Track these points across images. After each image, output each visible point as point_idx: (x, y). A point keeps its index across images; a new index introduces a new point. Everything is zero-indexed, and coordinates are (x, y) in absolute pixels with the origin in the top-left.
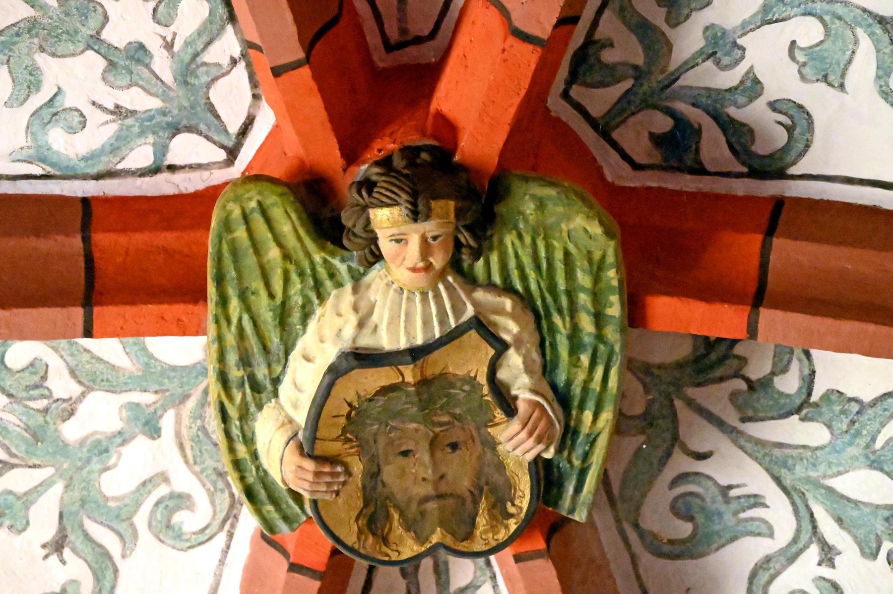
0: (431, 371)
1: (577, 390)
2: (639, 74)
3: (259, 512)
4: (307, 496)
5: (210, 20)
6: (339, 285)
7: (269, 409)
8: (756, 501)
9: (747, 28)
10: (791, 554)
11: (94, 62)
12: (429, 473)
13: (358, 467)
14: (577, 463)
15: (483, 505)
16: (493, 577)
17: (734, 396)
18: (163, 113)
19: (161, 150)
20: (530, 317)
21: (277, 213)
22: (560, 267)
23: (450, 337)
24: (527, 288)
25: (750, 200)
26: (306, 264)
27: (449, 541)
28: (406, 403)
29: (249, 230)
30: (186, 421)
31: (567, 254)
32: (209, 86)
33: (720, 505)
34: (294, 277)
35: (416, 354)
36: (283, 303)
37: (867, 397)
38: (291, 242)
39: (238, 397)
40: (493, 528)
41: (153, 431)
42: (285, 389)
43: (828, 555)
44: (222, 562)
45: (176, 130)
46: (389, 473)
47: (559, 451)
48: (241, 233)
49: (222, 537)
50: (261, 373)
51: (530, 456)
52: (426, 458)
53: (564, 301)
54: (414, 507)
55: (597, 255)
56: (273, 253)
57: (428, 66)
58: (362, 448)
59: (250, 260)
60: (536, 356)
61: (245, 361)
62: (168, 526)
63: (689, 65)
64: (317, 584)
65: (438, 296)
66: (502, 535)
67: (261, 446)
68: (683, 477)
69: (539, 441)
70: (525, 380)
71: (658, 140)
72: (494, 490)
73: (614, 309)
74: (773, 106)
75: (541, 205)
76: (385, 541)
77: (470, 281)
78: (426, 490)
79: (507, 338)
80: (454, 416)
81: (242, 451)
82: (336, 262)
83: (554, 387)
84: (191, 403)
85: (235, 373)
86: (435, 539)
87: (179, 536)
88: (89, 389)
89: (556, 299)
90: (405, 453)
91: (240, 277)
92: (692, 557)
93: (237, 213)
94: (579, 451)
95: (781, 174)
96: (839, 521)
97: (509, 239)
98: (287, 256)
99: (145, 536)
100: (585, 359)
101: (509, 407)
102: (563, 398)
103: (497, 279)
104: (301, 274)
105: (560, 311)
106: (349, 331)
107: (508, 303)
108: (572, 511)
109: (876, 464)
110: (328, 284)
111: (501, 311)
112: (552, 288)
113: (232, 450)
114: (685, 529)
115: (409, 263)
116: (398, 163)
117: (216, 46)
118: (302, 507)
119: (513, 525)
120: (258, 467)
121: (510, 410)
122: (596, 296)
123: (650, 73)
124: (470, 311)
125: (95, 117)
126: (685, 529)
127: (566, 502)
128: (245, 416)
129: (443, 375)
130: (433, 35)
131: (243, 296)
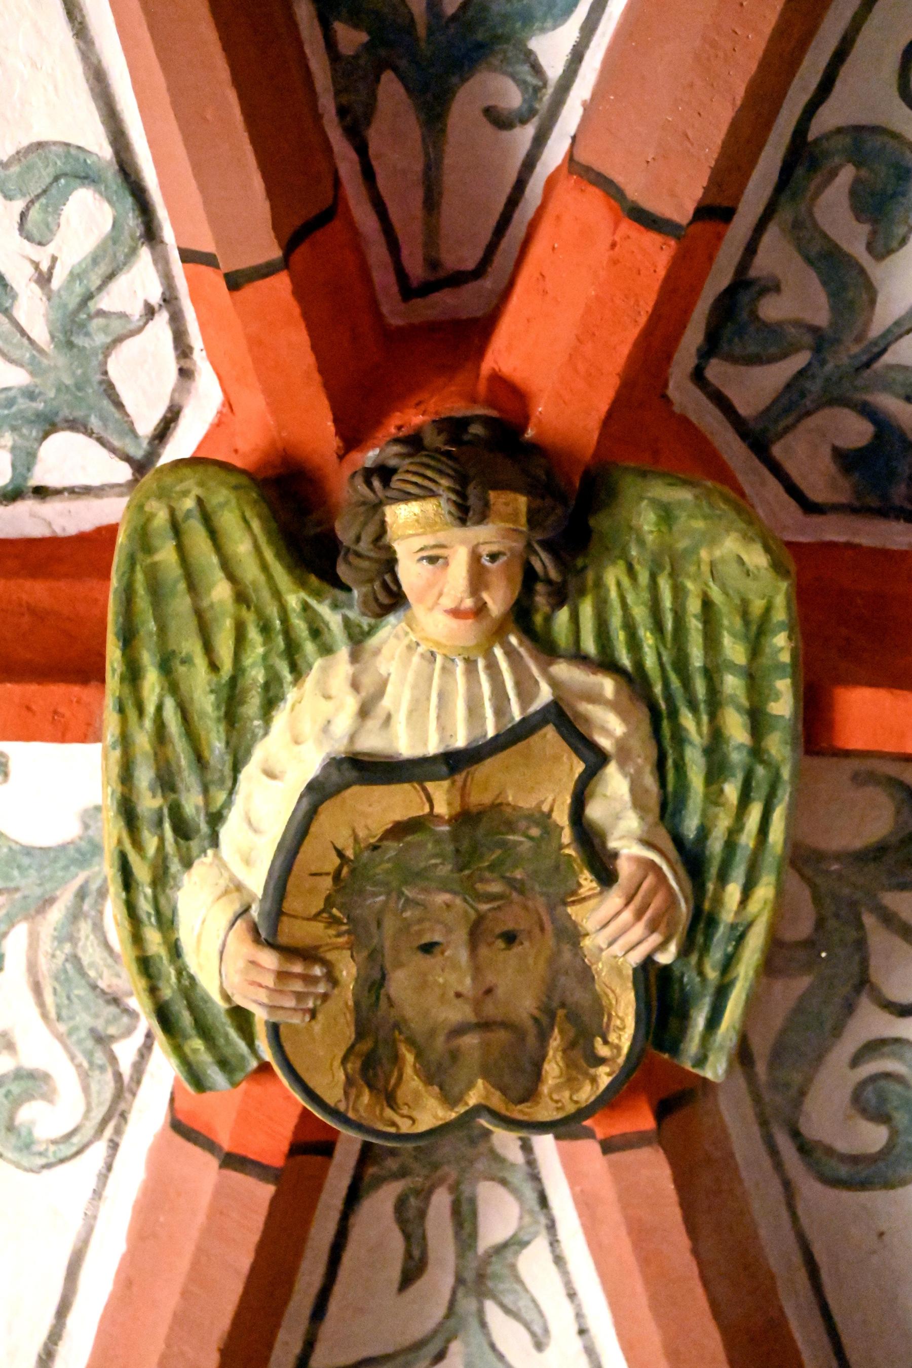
0: (479, 798)
1: (716, 846)
3: (178, 1050)
4: (260, 1016)
5: (114, 237)
6: (327, 650)
7: (203, 866)
12: (467, 984)
14: (712, 974)
15: (555, 1042)
16: (551, 1227)
18: (30, 394)
20: (642, 715)
22: (695, 625)
24: (639, 664)
26: (272, 611)
27: (497, 1101)
29: (181, 549)
30: (46, 944)
31: (707, 604)
32: (108, 350)
34: (253, 634)
36: (233, 681)
38: (250, 572)
39: (151, 844)
40: (570, 1082)
44: (98, 1194)
47: (684, 952)
48: (167, 554)
49: (100, 1149)
51: (636, 957)
52: (463, 955)
53: (700, 687)
54: (440, 1041)
55: (757, 606)
57: (474, 321)
59: (181, 604)
60: (650, 781)
62: (11, 1128)
64: (267, 1190)
65: (492, 667)
66: (586, 1094)
67: (186, 934)
69: (653, 928)
72: (573, 1017)
75: (667, 515)
76: (391, 1100)
79: (605, 743)
80: (511, 883)
81: (153, 939)
82: (323, 609)
83: (678, 840)
84: (56, 914)
86: (473, 1099)
87: (27, 1146)
89: (686, 682)
90: (428, 948)
91: (162, 629)
92: (889, 1185)
93: (162, 517)
94: (716, 955)
97: (613, 575)
98: (241, 597)
100: (731, 791)
103: (589, 646)
104: (265, 629)
105: (693, 706)
106: (344, 722)
107: (608, 685)
108: (701, 1061)
110: (309, 647)
111: (595, 698)
112: (681, 664)
113: (137, 939)
115: (448, 602)
116: (433, 439)
117: (122, 282)
118: (249, 1037)
119: (604, 1077)
120: (181, 971)
123: (837, 341)
124: (545, 694)
127: (692, 1045)
129: (497, 807)
130: (479, 272)
131: (166, 666)
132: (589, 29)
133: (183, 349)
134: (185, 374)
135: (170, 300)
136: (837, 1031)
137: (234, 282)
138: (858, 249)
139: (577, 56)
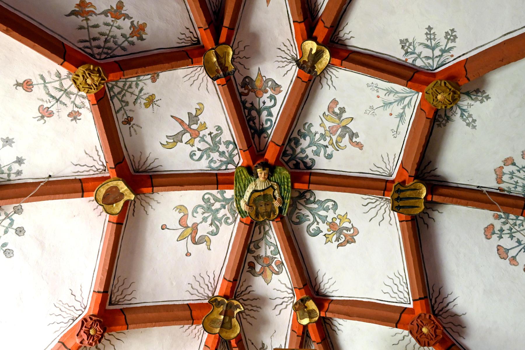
0: (265, 193)
1: (285, 197)
2: (292, 155)
3: (241, 215)
4: (247, 212)
5: (233, 148)
6: (252, 181)
7: (242, 199)
8: (308, 216)
9: (306, 148)
10: (313, 223)
11: (218, 154)
12: (264, 209)
13: (255, 208)
14: (285, 207)
15: (272, 213)
16: (271, 229)
17: (305, 201)
18: (227, 161)
19: (227, 166)
20: (278, 186)
21: (244, 171)
22: (282, 179)
23: (268, 188)
24: (278, 182)
25: (307, 173)
26: (248, 178)
27: (267, 218)
28: (261, 198)
29: (240, 173)
30: (229, 207)
31: (283, 177)
32: (233, 157)
33: (303, 217)
34: (246, 180)
35: (263, 190)
36: (245, 184)
37: (323, 200)
38: (246, 175)
39: (238, 198)
40: (273, 216)
41: (225, 208)
42: (245, 196)
43: (318, 223)
44: (234, 227)
45: (229, 164)
46: (259, 209)
47: (282, 205)
48: (239, 174)
49: (234, 224)
50: (241, 194)
51: (278, 206)
52: (264, 206)
53: (283, 183)
54: (262, 214)
55: (288, 177)
56: (243, 177)
58: (255, 204)
59: (240, 178)
60: (279, 191)
61: (239, 193)
62: (226, 222)
63: (299, 154)
64: (248, 226)
65: (266, 182)
66: (275, 217)
67: (241, 205)
68: (298, 213)
69: (280, 203)
70: (278, 195)
71: (294, 164)
72: (273, 211)
73: (290, 185)
74: (310, 159)
75: (280, 169)
76: (258, 218)
77: (270, 181)
78: (264, 211)
79: (275, 188)
80: (268, 200)
82: (252, 178)
83: (281, 196)
84: (230, 204)
85: (238, 194)
86: (265, 218)
87: (228, 223)
88: (216, 202)
89: (282, 183)
90: (261, 206)
91: (239, 180)
93: (238, 171)
94: (285, 206)
95: (311, 169)
96: (319, 218)
97: (276, 175)
98: (245, 177)
99: (223, 223)
100: (286, 192)
101: (275, 199)
102: (283, 198)
103: (274, 180)
104: (247, 180)
105: (282, 185)
106: (254, 187)
107: (275, 184)
108: (284, 214)
109: (324, 210)
110: (251, 181)
111: (275, 185)
112: (281, 182)
113: (237, 206)
114: (298, 220)
115: (262, 177)
116: (260, 164)
117: (234, 152)
118: (246, 213)
119: (276, 216)
120: (241, 208)
121: (276, 199)
122: (288, 183)
123: (293, 155)
124: (270, 184)
125: (218, 162)
126: (298, 220)
127: (283, 213)
128: (239, 201)
129: (267, 194)
131: (239, 183)
132: (272, 130)
133: (239, 157)
134: (240, 159)
135: (238, 153)
136: (295, 212)
137: (244, 151)
138: (294, 147)
139: (271, 132)
